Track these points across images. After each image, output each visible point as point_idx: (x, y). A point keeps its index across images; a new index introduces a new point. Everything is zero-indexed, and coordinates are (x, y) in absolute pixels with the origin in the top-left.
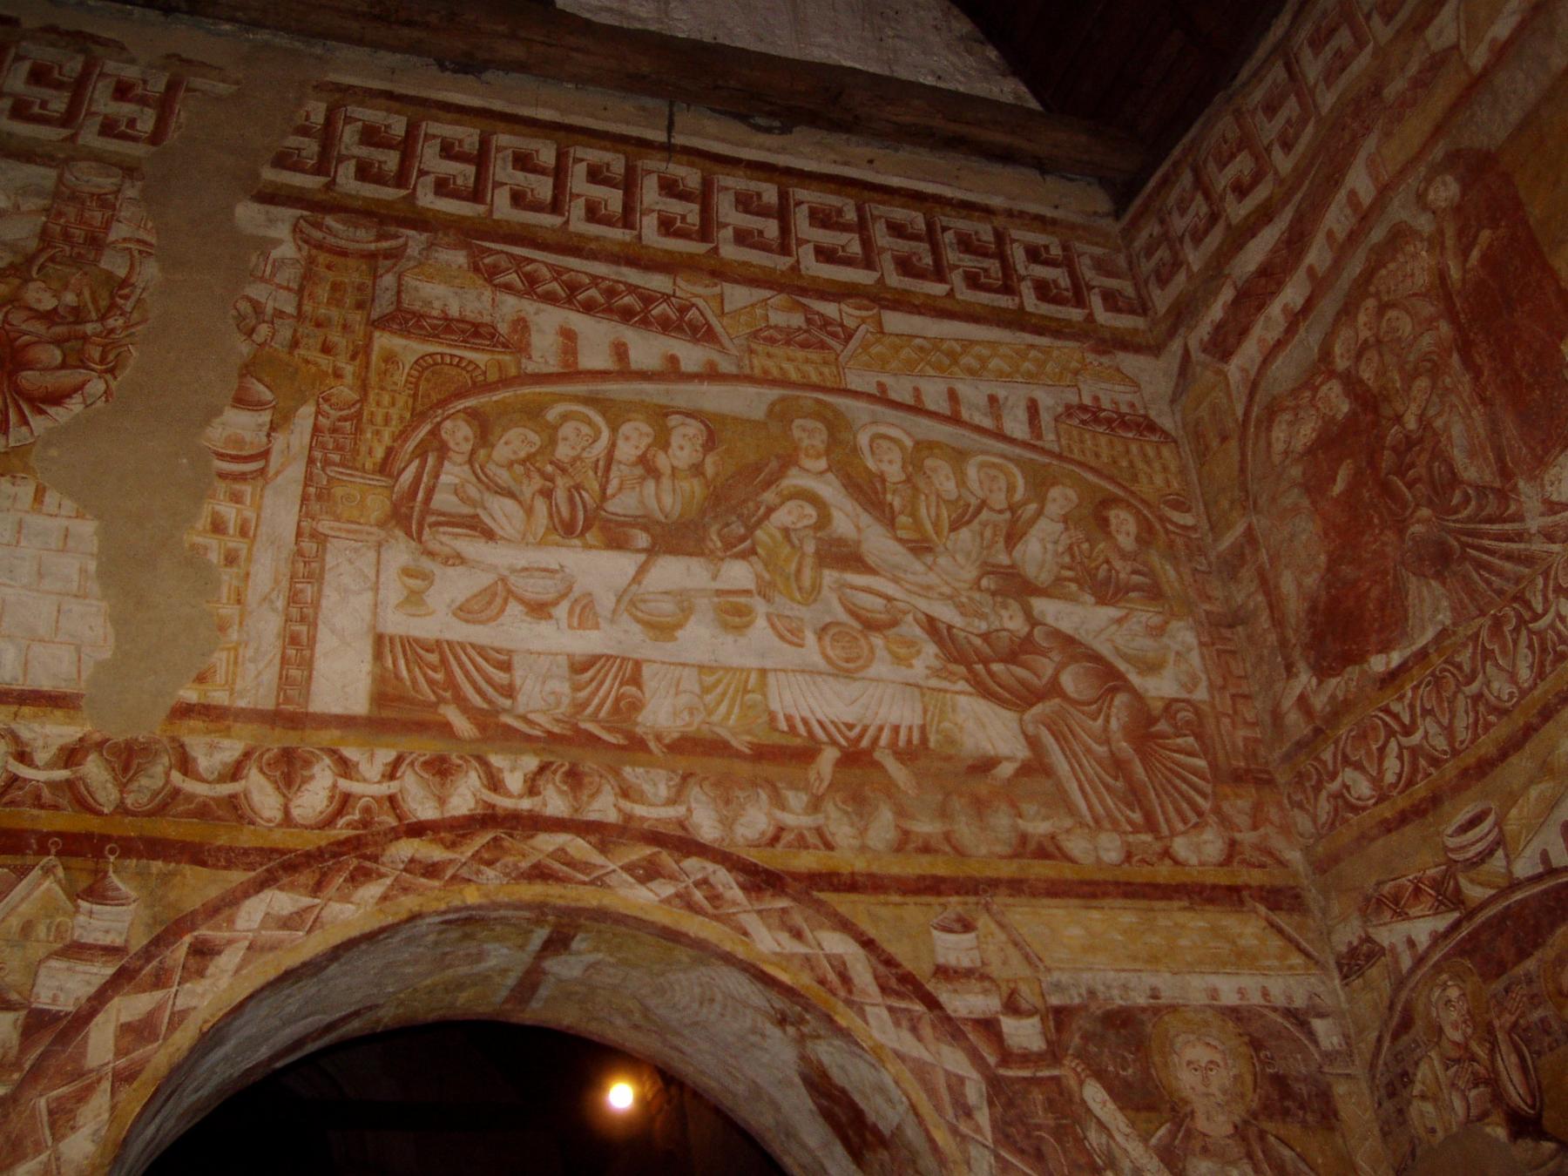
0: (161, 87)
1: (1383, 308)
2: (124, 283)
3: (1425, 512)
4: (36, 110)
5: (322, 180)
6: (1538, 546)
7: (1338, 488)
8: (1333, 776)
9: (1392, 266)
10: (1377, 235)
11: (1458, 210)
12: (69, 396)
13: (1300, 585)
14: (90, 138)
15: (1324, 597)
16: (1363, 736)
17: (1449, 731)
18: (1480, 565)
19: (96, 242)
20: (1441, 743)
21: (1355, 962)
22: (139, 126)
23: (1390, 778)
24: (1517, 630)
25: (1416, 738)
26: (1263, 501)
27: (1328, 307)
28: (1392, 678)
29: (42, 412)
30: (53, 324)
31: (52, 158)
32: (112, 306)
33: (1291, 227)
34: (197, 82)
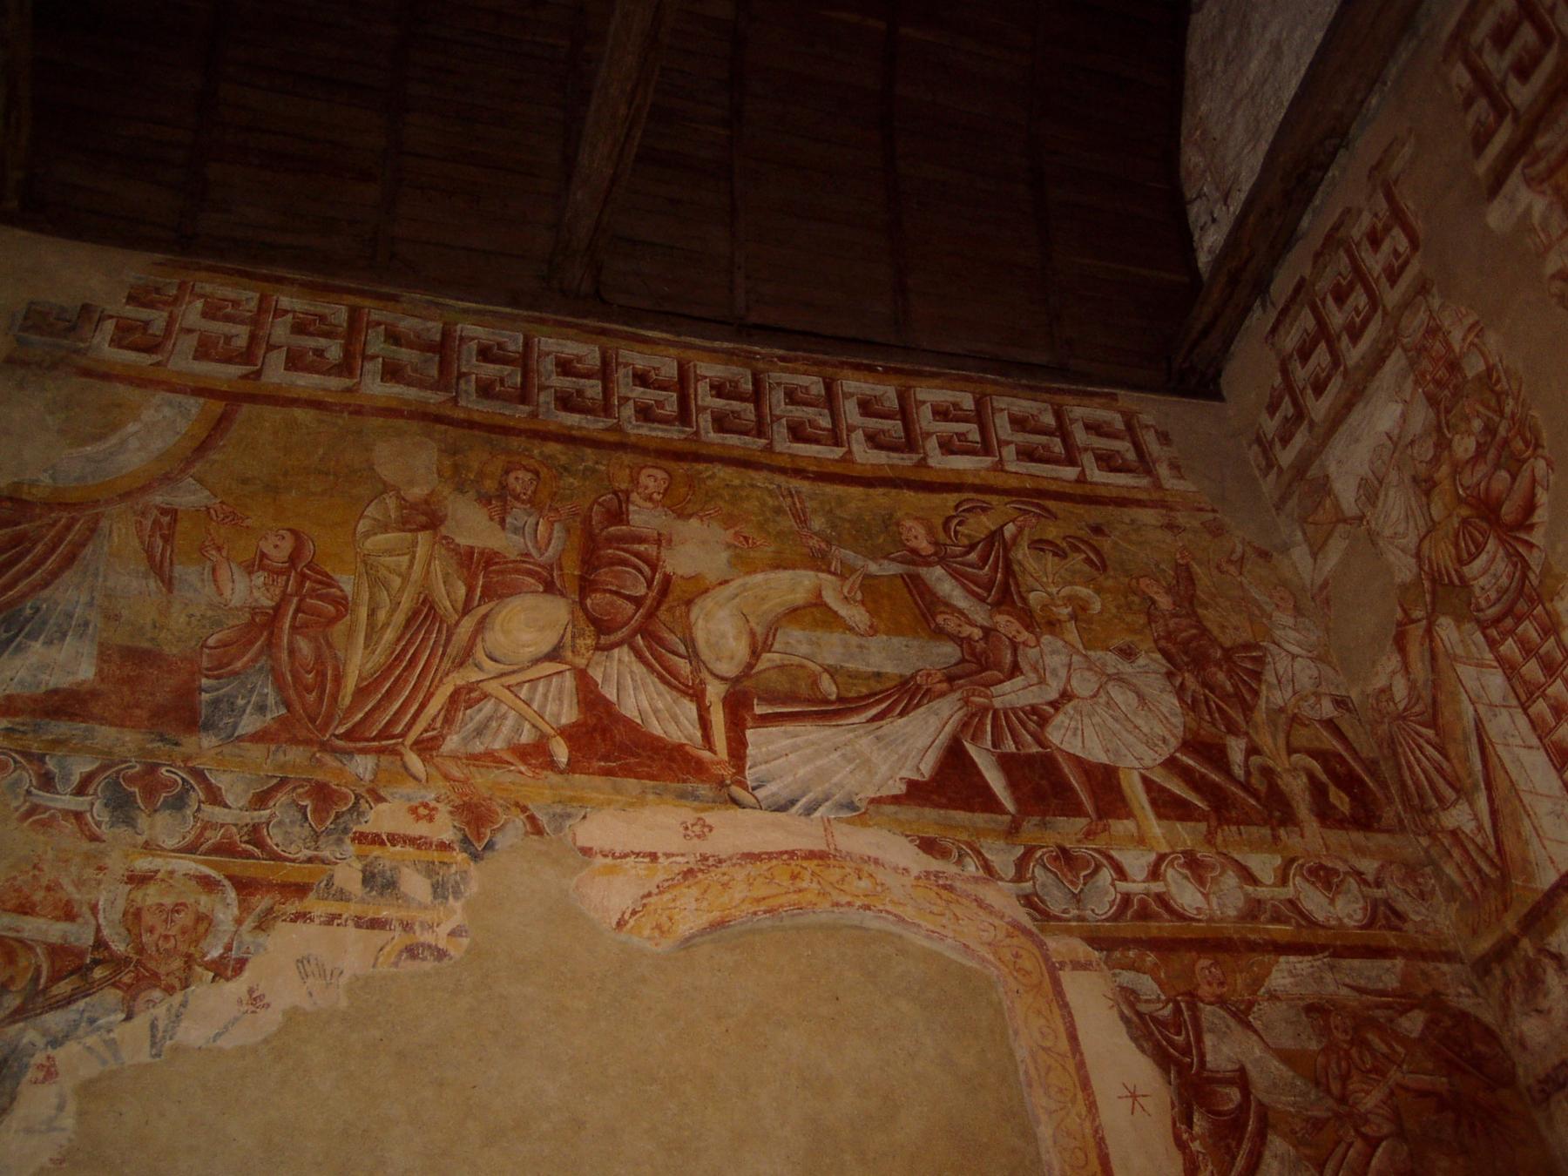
0: (1385, 205)
2: (1490, 370)
4: (1358, 320)
5: (1509, 118)
12: (1533, 495)
14: (1392, 297)
19: (1454, 366)
22: (1401, 249)
29: (1531, 527)
30: (1486, 452)
31: (1389, 341)
32: (1498, 395)
34: (1396, 167)
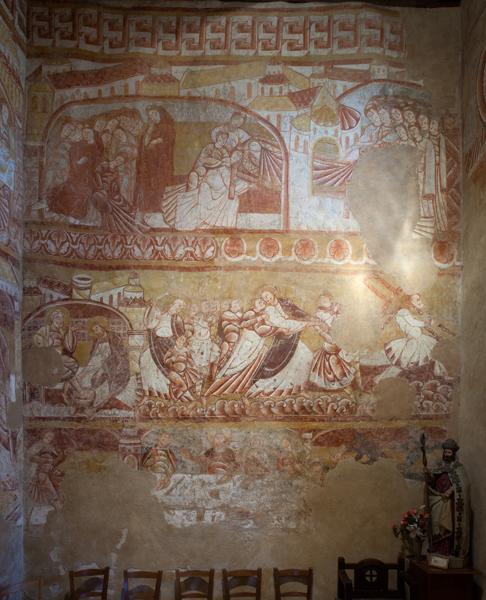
1: (118, 127)
3: (105, 192)
6: (136, 228)
7: (80, 162)
8: (43, 239)
9: (129, 119)
10: (128, 105)
11: (156, 125)
13: (54, 178)
15: (61, 189)
16: (59, 236)
17: (86, 252)
18: (115, 219)
20: (83, 253)
21: (27, 291)
23: (62, 251)
24: (119, 243)
25: (76, 247)
26: (52, 144)
27: (99, 108)
28: (75, 226)
33: (100, 71)
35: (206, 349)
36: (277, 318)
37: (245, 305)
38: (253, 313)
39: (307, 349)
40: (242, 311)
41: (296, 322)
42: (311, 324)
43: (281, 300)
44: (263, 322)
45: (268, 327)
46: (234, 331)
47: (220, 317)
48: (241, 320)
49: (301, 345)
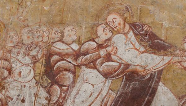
35: (28, 94)
36: (129, 52)
37: (84, 34)
38: (93, 44)
39: (171, 95)
40: (79, 41)
41: (155, 56)
42: (176, 59)
43: (134, 26)
44: (108, 58)
45: (116, 64)
46: (68, 70)
47: (49, 50)
48: (77, 55)
49: (162, 88)
